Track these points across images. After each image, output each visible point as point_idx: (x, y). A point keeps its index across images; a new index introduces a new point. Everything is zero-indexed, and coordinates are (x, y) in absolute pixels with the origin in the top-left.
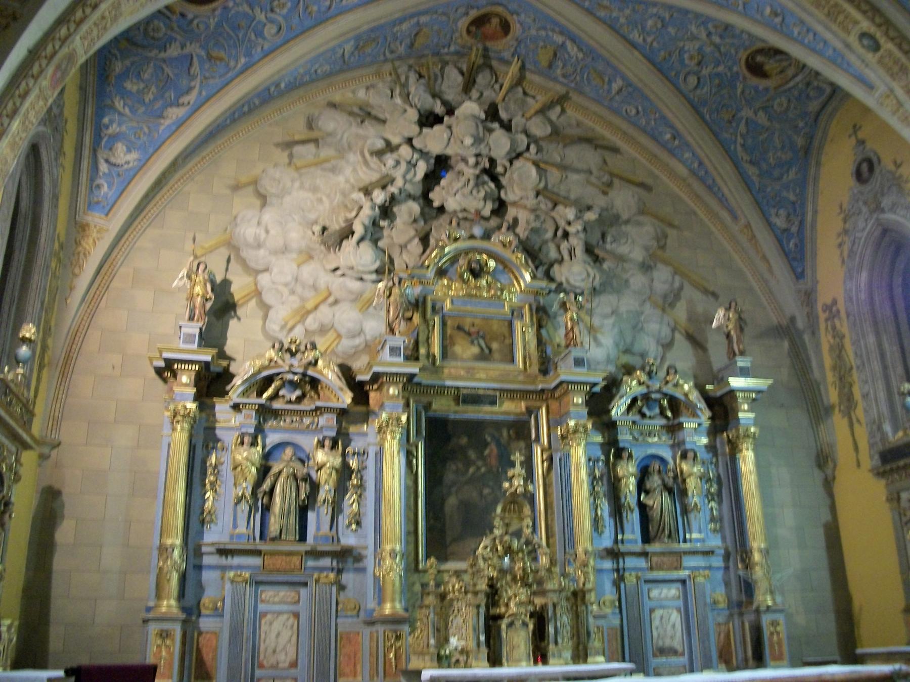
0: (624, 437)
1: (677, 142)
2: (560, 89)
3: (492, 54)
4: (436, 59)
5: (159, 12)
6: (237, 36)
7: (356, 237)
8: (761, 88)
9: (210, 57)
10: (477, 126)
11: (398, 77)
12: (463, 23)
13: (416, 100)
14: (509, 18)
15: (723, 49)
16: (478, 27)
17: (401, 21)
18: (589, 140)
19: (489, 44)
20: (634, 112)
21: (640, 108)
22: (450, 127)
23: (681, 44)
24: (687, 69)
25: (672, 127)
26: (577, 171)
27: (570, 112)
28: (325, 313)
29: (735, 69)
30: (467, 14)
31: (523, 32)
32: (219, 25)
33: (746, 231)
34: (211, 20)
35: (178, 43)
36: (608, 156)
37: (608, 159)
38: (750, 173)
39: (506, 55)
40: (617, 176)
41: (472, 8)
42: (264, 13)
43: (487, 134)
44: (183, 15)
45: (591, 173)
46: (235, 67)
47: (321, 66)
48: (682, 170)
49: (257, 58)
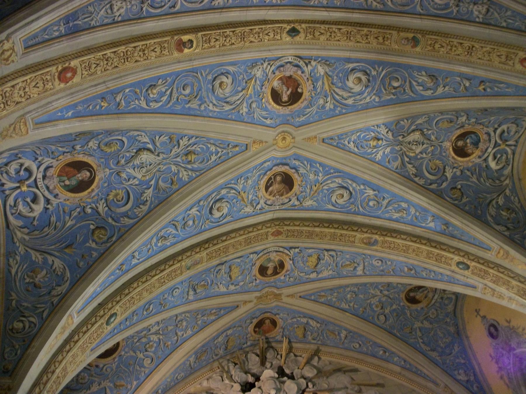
1: (387, 354)
2: (314, 347)
3: (271, 340)
4: (241, 352)
5: (85, 368)
6: (130, 370)
8: (419, 309)
9: (116, 386)
10: (275, 383)
11: (223, 368)
12: (251, 328)
13: (237, 378)
14: (274, 318)
15: (391, 297)
16: (259, 328)
17: (218, 337)
18: (339, 370)
19: (267, 335)
20: (358, 346)
21: (360, 343)
22: (260, 388)
23: (369, 301)
24: (377, 313)
25: (380, 346)
26: (339, 390)
27: (323, 358)
29: (402, 304)
31: (284, 323)
32: (117, 367)
33: (446, 390)
34: (113, 365)
35: (96, 383)
36: (353, 375)
37: (353, 376)
38: (434, 356)
39: (279, 338)
41: (253, 318)
43: (282, 385)
44: (97, 366)
45: (347, 388)
46: (131, 388)
47: (179, 374)
48: (398, 369)
49: (142, 379)
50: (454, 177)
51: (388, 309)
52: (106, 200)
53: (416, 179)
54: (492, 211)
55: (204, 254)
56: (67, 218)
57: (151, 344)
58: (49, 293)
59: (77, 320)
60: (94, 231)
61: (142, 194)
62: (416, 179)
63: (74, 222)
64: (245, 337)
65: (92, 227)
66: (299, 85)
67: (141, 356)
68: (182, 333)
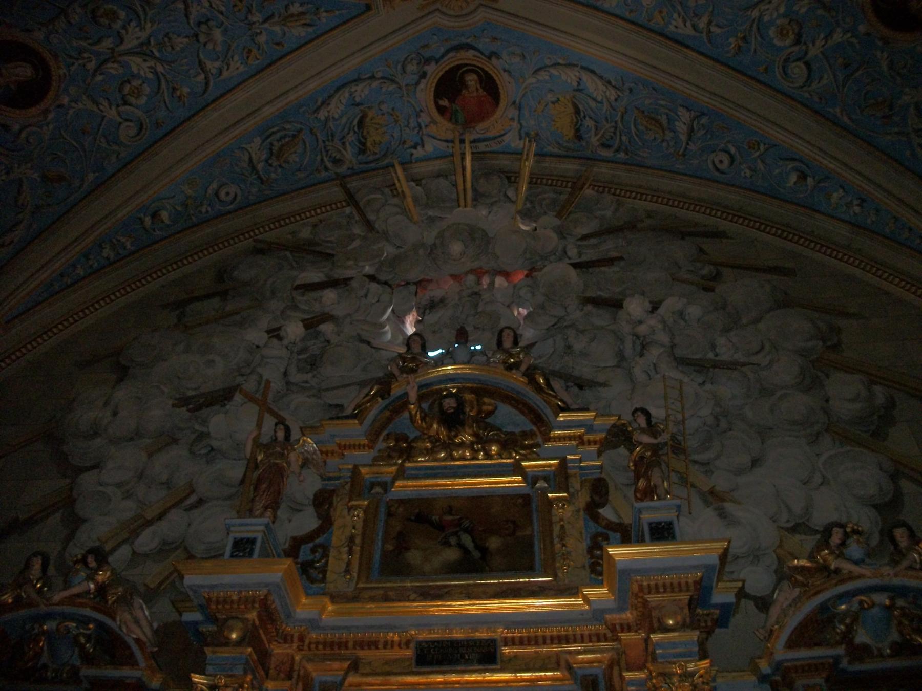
28: (174, 524)
29: (862, 28)
30: (424, 75)
37: (705, 247)
40: (722, 264)
41: (428, 61)
42: (114, 108)
51: (819, 43)
57: (136, 83)
64: (413, 124)
67: (112, 113)
68: (217, 64)
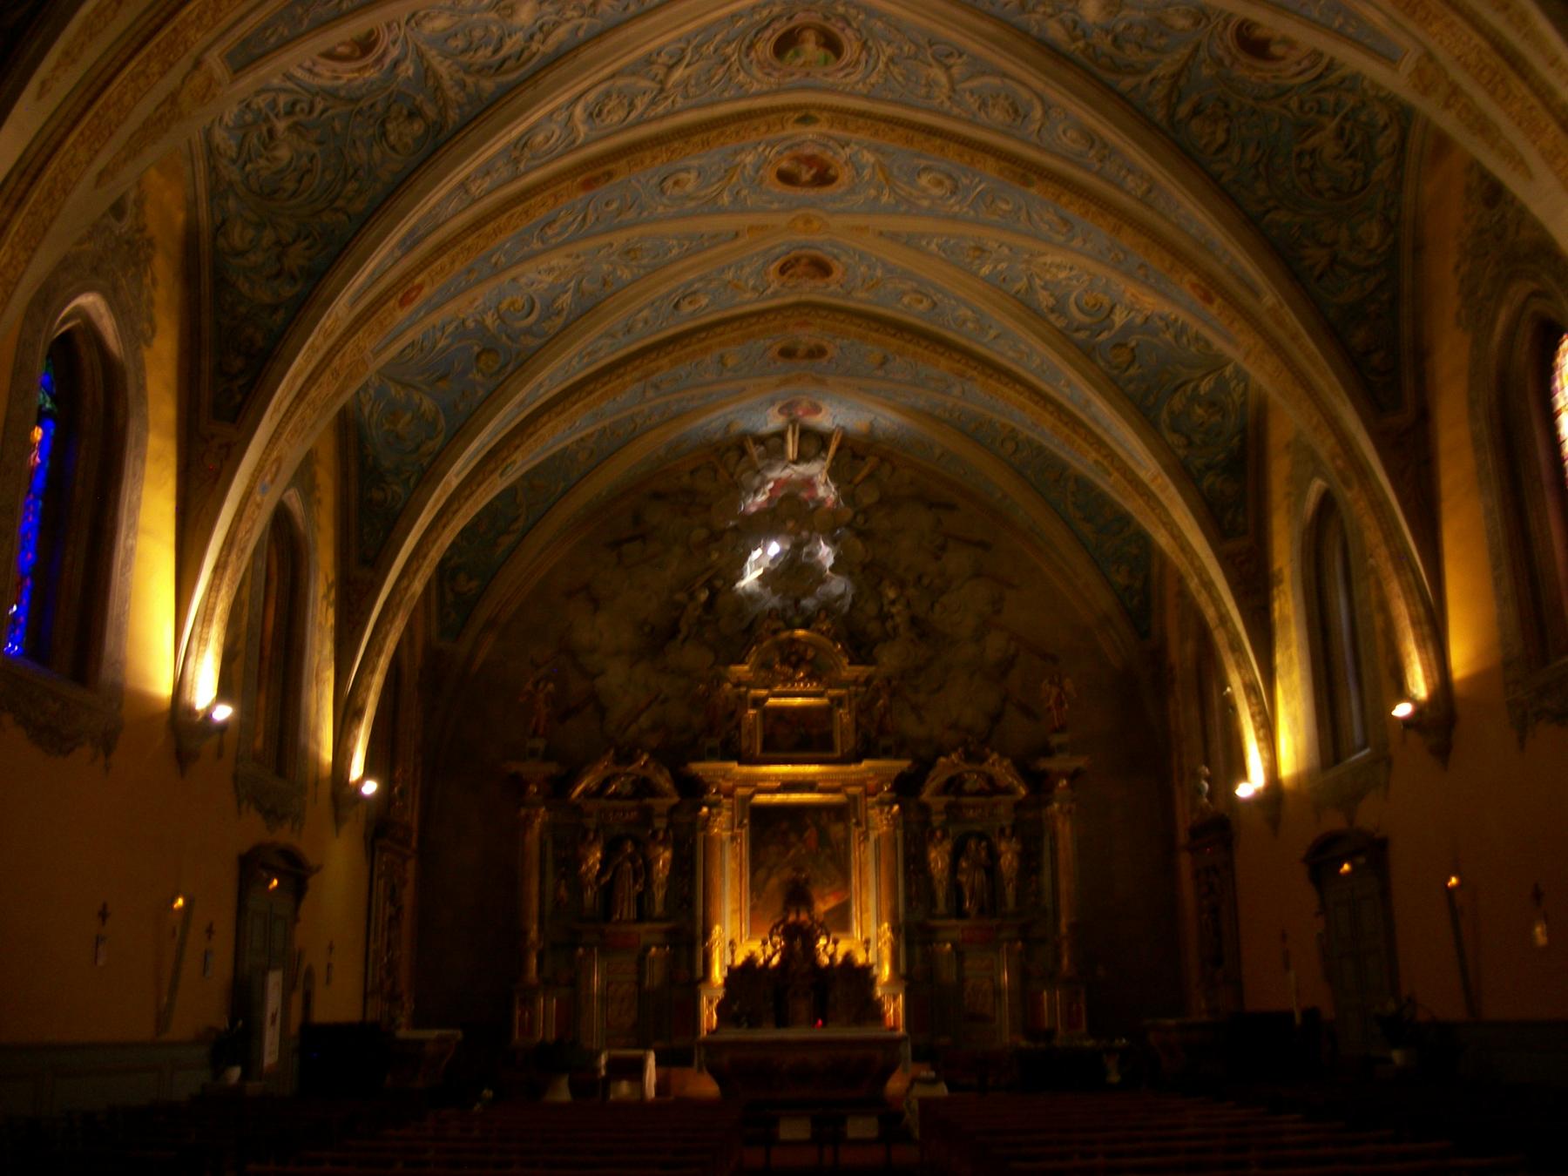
0: (937, 820)
7: (681, 637)
50: (1128, 329)
52: (498, 311)
53: (1052, 318)
54: (1178, 402)
55: (665, 361)
56: (439, 334)
58: (418, 447)
59: (455, 483)
60: (478, 356)
61: (554, 301)
62: (1052, 318)
63: (448, 341)
65: (476, 349)
66: (828, 168)
